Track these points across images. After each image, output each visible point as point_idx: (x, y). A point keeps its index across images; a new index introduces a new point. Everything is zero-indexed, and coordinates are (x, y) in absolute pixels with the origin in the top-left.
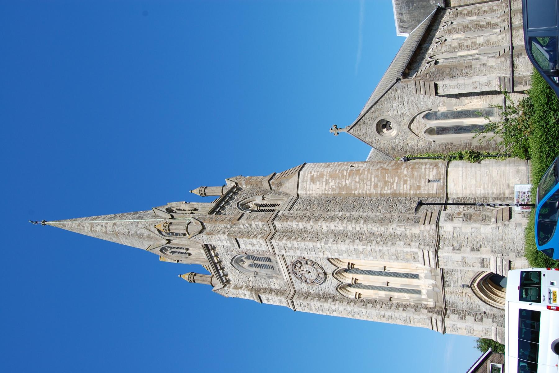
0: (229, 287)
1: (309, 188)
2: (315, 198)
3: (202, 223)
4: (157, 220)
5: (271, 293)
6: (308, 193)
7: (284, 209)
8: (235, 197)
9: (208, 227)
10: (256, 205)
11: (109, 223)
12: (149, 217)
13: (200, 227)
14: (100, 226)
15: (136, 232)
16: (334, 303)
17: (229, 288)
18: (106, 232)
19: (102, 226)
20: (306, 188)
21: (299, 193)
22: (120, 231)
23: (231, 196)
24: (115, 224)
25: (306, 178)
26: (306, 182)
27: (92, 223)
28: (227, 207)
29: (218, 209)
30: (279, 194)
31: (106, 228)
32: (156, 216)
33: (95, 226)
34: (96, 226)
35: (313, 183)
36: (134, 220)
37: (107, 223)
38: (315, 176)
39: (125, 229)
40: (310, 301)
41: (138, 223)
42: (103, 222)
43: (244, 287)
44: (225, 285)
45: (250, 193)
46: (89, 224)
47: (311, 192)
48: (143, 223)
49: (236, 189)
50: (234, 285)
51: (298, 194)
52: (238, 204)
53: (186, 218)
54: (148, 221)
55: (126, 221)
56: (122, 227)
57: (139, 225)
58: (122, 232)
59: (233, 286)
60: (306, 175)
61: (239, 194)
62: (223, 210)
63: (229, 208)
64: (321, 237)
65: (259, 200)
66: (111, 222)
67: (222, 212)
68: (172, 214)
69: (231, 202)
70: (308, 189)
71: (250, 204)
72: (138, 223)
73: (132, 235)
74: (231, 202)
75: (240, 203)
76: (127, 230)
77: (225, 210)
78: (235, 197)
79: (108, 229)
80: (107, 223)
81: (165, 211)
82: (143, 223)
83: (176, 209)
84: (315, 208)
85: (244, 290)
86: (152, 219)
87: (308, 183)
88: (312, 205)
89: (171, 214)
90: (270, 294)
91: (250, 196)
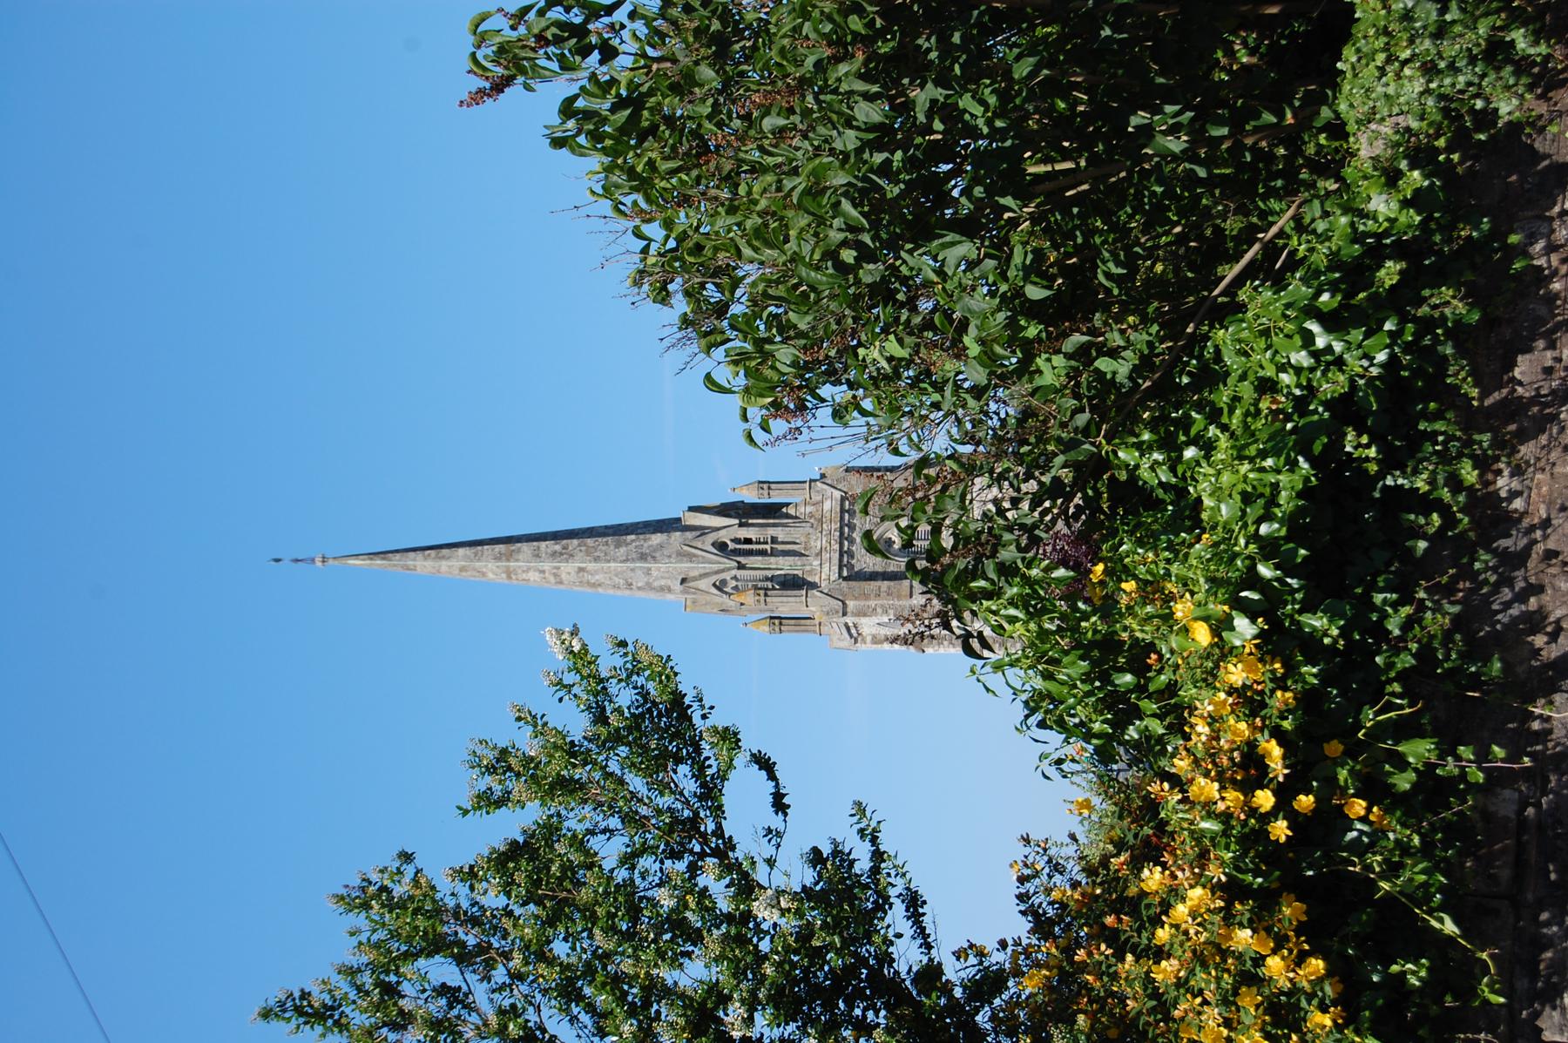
0: (864, 641)
15: (648, 584)
18: (561, 583)
19: (543, 572)
24: (581, 570)
27: (508, 567)
31: (555, 575)
32: (691, 557)
37: (558, 568)
41: (650, 569)
55: (612, 565)
57: (654, 573)
59: (869, 639)
62: (853, 557)
66: (568, 569)
69: (854, 535)
72: (650, 569)
73: (639, 588)
79: (564, 576)
83: (732, 540)
86: (681, 562)
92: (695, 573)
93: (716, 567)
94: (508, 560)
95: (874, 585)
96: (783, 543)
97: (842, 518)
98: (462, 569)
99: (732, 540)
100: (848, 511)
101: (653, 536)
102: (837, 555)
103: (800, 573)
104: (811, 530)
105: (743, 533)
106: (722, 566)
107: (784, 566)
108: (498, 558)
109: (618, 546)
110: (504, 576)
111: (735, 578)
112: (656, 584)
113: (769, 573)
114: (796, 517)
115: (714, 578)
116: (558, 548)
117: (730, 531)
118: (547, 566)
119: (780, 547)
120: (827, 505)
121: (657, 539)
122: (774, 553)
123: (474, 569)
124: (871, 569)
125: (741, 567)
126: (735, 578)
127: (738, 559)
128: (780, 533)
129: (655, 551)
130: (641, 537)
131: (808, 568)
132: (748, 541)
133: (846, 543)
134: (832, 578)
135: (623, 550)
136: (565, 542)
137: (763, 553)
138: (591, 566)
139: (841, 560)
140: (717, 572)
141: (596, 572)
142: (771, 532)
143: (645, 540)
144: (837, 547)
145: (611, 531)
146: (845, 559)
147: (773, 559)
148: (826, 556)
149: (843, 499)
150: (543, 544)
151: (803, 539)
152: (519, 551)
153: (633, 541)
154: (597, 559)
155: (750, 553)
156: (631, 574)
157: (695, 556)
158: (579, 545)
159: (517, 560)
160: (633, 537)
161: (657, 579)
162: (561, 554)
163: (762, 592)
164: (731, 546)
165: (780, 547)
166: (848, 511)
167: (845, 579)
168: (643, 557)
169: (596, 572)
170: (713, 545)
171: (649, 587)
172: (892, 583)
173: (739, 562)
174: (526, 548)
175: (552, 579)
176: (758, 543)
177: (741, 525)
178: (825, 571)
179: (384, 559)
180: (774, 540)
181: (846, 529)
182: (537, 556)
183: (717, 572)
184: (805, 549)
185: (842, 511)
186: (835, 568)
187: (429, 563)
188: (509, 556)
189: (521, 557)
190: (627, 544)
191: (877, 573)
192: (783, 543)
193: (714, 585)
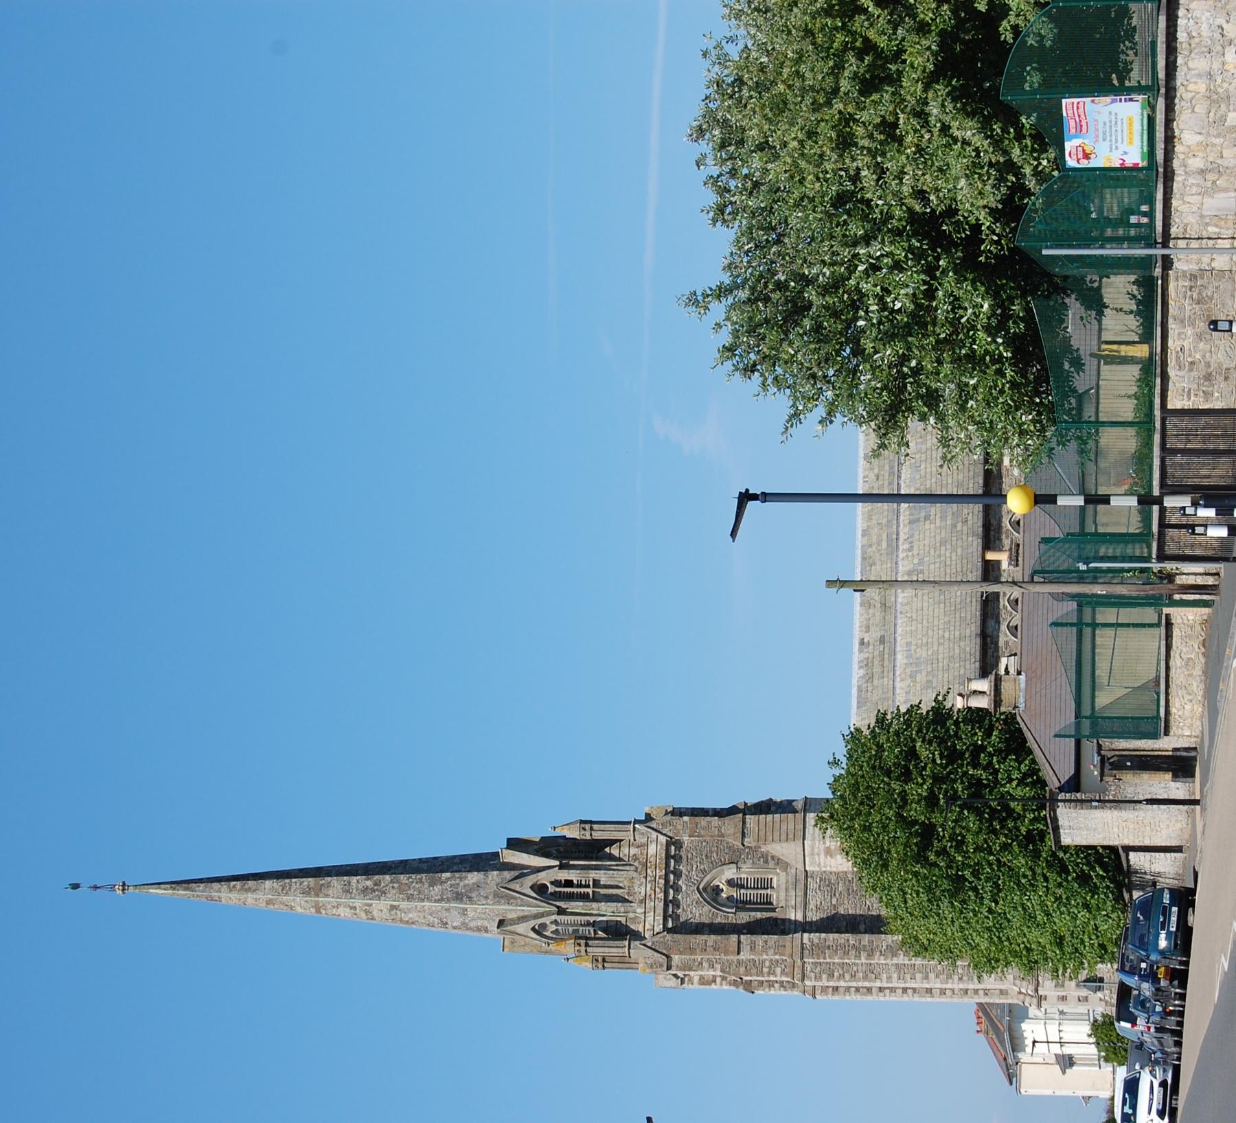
1: (825, 863)
2: (837, 874)
3: (667, 957)
4: (519, 908)
5: (773, 986)
6: (824, 869)
7: (793, 903)
8: (681, 867)
9: (676, 959)
10: (730, 883)
11: (374, 905)
12: (487, 898)
13: (663, 959)
14: (344, 907)
15: (463, 923)
16: (881, 994)
17: (692, 984)
18: (373, 919)
19: (355, 908)
20: (820, 864)
21: (807, 869)
22: (417, 919)
23: (674, 868)
24: (393, 907)
25: (816, 851)
26: (819, 855)
28: (679, 897)
29: (671, 910)
30: (765, 857)
31: (367, 912)
32: (509, 900)
33: (329, 907)
34: (334, 907)
35: (831, 856)
36: (452, 905)
37: (371, 905)
38: (832, 848)
39: (429, 917)
40: (845, 994)
42: (353, 902)
43: (718, 979)
44: (682, 979)
45: (704, 854)
46: (306, 901)
47: (828, 869)
48: (478, 911)
49: (673, 848)
50: (698, 977)
51: (806, 871)
52: (698, 888)
53: (592, 909)
54: (493, 909)
55: (426, 904)
56: (419, 914)
57: (471, 914)
58: (423, 921)
60: (817, 846)
61: (684, 857)
62: (678, 907)
63: (685, 899)
64: (878, 970)
65: (730, 873)
66: (380, 907)
67: (678, 912)
68: (558, 904)
69: (680, 883)
70: (822, 864)
71: (716, 882)
73: (454, 928)
74: (680, 883)
75: (701, 887)
76: (436, 919)
77: (681, 907)
78: (681, 867)
79: (375, 913)
80: (371, 905)
81: (535, 895)
82: (478, 911)
83: (552, 883)
84: (846, 902)
85: (721, 985)
86: (499, 903)
87: (822, 856)
88: (837, 895)
89: (555, 903)
90: (772, 988)
91: (711, 865)
92: (513, 915)
93: (535, 910)
94: (317, 895)
95: (700, 938)
96: (606, 887)
97: (667, 865)
98: (269, 902)
99: (552, 883)
100: (673, 857)
101: (470, 875)
102: (662, 904)
103: (623, 920)
104: (635, 874)
105: (564, 875)
106: (541, 910)
107: (607, 911)
108: (306, 893)
109: (432, 884)
110: (313, 910)
111: (556, 922)
112: (472, 924)
113: (592, 919)
114: (620, 859)
115: (532, 923)
116: (369, 883)
117: (551, 872)
118: (358, 902)
119: (603, 891)
120: (652, 849)
121: (473, 877)
122: (596, 898)
123: (282, 903)
124: (697, 920)
125: (561, 911)
126: (556, 922)
127: (558, 904)
128: (602, 876)
129: (471, 891)
130: (457, 875)
131: (631, 915)
132: (569, 883)
133: (671, 891)
134: (657, 929)
135: (437, 888)
136: (377, 877)
137: (584, 897)
138: (404, 905)
139: (665, 910)
140: (536, 916)
141: (410, 910)
142: (593, 874)
143: (461, 879)
144: (661, 895)
145: (425, 866)
146: (671, 910)
147: (594, 905)
148: (650, 904)
149: (668, 845)
150: (354, 879)
151: (626, 883)
152: (329, 885)
153: (448, 879)
154: (410, 898)
155: (571, 897)
156: (446, 914)
157: (515, 898)
158: (392, 882)
159: (327, 896)
160: (448, 875)
161: (473, 919)
162: (374, 891)
163: (583, 942)
164: (551, 889)
165: (603, 891)
166: (673, 857)
167: (669, 931)
168: (458, 897)
169: (410, 910)
170: (532, 888)
171: (465, 926)
172: (719, 937)
173: (558, 907)
174: (336, 883)
175: (363, 915)
176: (580, 886)
177: (561, 867)
178: (648, 921)
179: (186, 889)
180: (596, 883)
181: (672, 877)
182: (348, 891)
183: (536, 916)
184: (628, 894)
185: (668, 856)
186: (660, 919)
187: (234, 895)
188: (318, 891)
189: (330, 892)
190: (442, 883)
191: (704, 924)
192: (606, 887)
193: (533, 929)
